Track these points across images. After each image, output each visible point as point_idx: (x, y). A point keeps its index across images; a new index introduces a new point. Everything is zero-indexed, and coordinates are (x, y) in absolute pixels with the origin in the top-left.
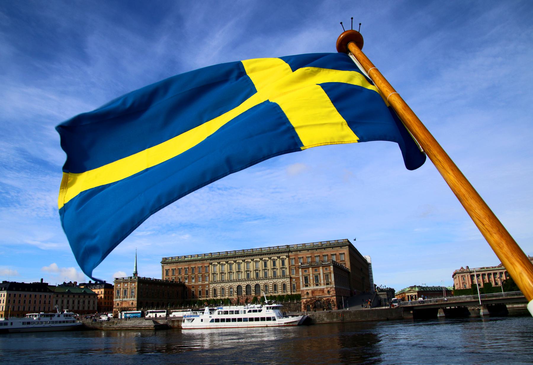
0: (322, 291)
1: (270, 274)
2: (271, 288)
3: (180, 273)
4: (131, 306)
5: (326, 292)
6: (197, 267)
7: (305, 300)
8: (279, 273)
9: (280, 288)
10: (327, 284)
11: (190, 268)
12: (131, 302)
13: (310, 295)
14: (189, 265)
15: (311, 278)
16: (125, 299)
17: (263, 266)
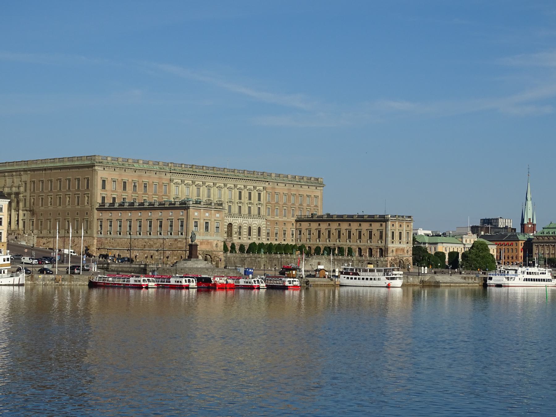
0: (403, 250)
1: (245, 210)
2: (245, 231)
3: (125, 188)
4: (215, 249)
5: (406, 251)
6: (151, 182)
7: (390, 258)
8: (254, 211)
9: (254, 232)
10: (408, 243)
11: (140, 181)
12: (215, 242)
13: (394, 253)
14: (140, 176)
15: (397, 234)
16: (208, 238)
17: (238, 198)
